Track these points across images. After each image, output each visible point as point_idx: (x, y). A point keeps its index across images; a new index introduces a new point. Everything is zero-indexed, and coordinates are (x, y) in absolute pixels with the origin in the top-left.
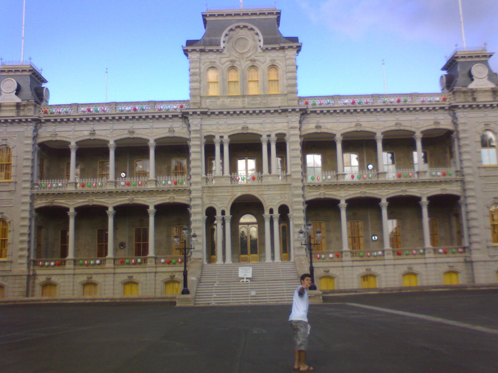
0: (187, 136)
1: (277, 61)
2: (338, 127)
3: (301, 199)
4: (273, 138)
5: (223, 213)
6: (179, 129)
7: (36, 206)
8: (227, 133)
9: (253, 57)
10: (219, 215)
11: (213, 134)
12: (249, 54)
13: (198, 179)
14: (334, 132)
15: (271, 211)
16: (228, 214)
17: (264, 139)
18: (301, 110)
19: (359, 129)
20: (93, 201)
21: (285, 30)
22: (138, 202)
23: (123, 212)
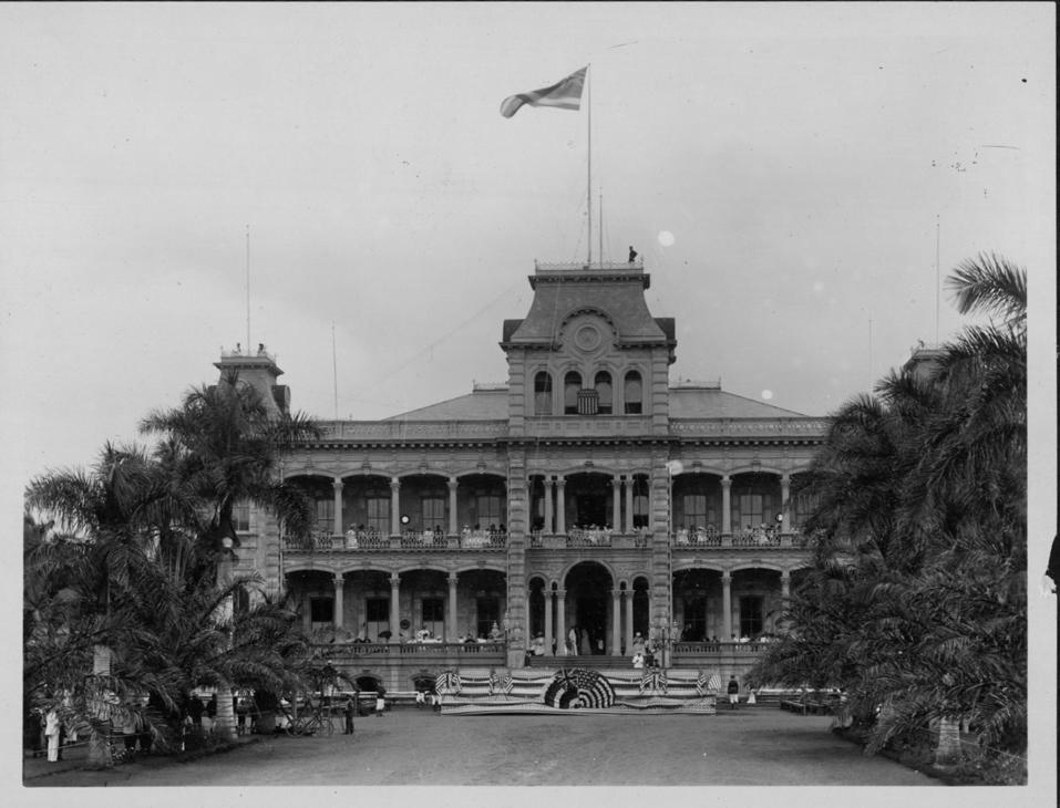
0: (503, 474)
1: (641, 366)
2: (723, 465)
3: (663, 569)
4: (630, 478)
5: (555, 586)
6: (493, 465)
7: (288, 571)
8: (561, 471)
9: (603, 358)
10: (548, 590)
11: (542, 473)
12: (599, 353)
13: (521, 537)
14: (721, 473)
15: (623, 586)
16: (562, 590)
17: (617, 478)
18: (669, 441)
19: (756, 469)
20: (370, 564)
21: (657, 302)
22: (435, 568)
23: (410, 580)
